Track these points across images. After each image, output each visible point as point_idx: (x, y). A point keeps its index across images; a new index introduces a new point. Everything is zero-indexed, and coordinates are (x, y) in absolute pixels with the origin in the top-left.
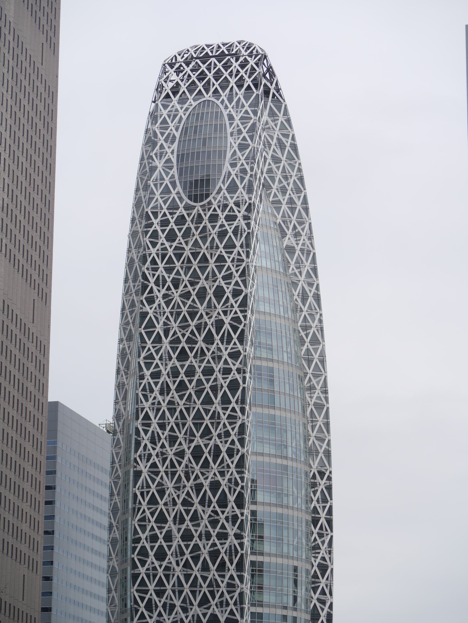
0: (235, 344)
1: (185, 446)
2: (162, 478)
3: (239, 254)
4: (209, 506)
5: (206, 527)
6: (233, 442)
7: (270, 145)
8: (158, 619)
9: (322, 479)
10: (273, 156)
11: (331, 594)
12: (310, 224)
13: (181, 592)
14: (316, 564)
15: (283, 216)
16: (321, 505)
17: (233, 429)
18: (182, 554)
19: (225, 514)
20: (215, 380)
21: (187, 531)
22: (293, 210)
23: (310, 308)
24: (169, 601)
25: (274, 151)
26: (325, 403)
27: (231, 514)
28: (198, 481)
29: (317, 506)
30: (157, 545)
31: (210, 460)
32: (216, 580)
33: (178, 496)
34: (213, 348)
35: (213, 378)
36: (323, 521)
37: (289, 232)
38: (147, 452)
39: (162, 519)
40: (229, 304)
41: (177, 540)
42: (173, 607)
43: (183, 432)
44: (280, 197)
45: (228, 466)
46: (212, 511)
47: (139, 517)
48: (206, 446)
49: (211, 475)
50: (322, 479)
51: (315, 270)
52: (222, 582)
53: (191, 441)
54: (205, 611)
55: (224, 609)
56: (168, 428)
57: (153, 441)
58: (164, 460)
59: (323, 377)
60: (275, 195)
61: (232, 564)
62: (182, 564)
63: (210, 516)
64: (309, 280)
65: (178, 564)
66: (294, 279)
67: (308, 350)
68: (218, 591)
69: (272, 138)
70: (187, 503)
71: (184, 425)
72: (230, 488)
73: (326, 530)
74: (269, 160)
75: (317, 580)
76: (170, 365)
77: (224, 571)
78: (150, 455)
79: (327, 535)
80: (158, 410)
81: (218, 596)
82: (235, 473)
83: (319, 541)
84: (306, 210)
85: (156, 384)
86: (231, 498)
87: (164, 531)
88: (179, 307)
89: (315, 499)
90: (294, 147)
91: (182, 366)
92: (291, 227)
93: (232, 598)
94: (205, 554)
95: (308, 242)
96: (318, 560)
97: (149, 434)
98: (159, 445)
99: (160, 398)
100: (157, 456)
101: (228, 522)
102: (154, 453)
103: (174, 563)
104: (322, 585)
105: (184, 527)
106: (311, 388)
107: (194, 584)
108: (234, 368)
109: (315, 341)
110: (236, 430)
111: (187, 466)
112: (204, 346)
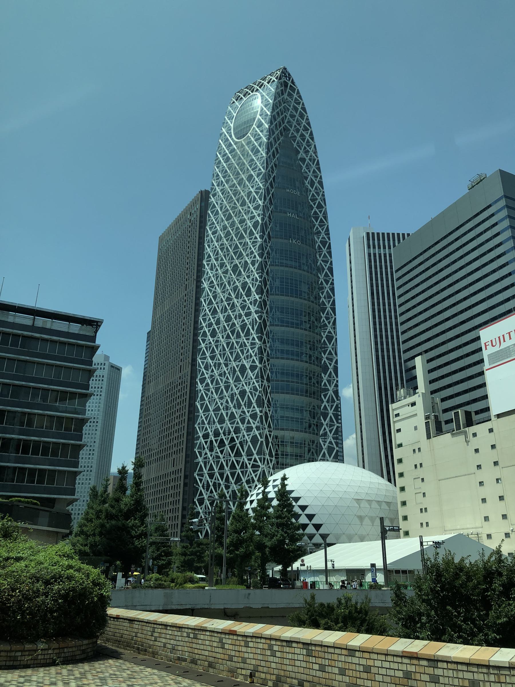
0: (257, 201)
1: (228, 267)
2: (215, 289)
3: (262, 154)
4: (241, 298)
5: (239, 311)
6: (255, 257)
7: (288, 110)
8: (211, 374)
9: (327, 285)
10: (290, 115)
11: (336, 354)
12: (315, 146)
13: (224, 354)
14: (324, 336)
15: (298, 143)
16: (327, 300)
17: (255, 249)
18: (226, 330)
19: (250, 300)
20: (246, 224)
21: (229, 316)
22: (304, 140)
23: (316, 188)
24: (217, 362)
25: (291, 112)
26: (328, 240)
27: (253, 299)
28: (235, 285)
29: (324, 300)
30: (211, 328)
31: (242, 270)
32: (244, 342)
33: (224, 297)
34: (245, 207)
35: (244, 224)
36: (329, 309)
37: (301, 151)
38: (208, 276)
39: (215, 312)
40: (255, 181)
41: (223, 323)
42: (220, 364)
43: (228, 259)
44: (296, 134)
45: (252, 271)
46: (243, 301)
47: (203, 314)
48: (240, 263)
49: (242, 279)
50: (327, 285)
51: (319, 169)
52: (248, 343)
53: (232, 263)
54: (238, 363)
55: (249, 360)
56: (220, 259)
57: (212, 269)
58: (217, 278)
59: (326, 226)
60: (292, 133)
61: (253, 330)
62: (225, 337)
63: (241, 304)
64: (315, 174)
65: (223, 338)
66: (305, 175)
67: (315, 212)
68: (245, 349)
69: (290, 106)
70: (228, 299)
71: (228, 255)
72: (253, 284)
73: (331, 315)
74: (288, 117)
75: (326, 346)
76: (222, 224)
77: (249, 335)
78: (210, 277)
79: (332, 317)
80: (215, 251)
81: (245, 352)
82: (256, 274)
83: (326, 322)
84: (312, 139)
85: (214, 237)
86: (253, 290)
87: (216, 319)
88: (229, 193)
89: (322, 296)
90: (304, 109)
91: (228, 223)
92: (303, 148)
93: (253, 352)
94: (238, 328)
95: (314, 155)
96: (326, 334)
97: (210, 265)
98: (214, 270)
99: (216, 244)
100: (213, 276)
101: (251, 305)
102: (211, 275)
103: (221, 337)
104: (330, 349)
105: (226, 314)
106: (319, 233)
107: (232, 348)
108: (256, 214)
109: (320, 206)
110: (257, 249)
111: (229, 278)
112: (240, 208)
